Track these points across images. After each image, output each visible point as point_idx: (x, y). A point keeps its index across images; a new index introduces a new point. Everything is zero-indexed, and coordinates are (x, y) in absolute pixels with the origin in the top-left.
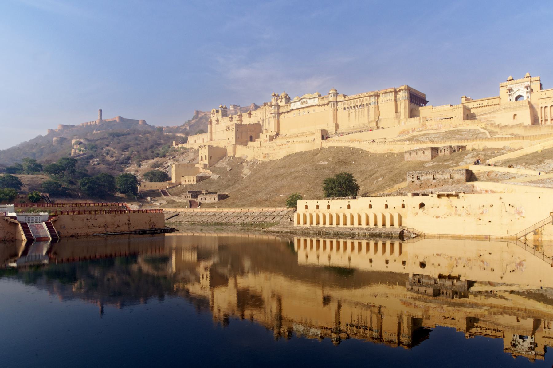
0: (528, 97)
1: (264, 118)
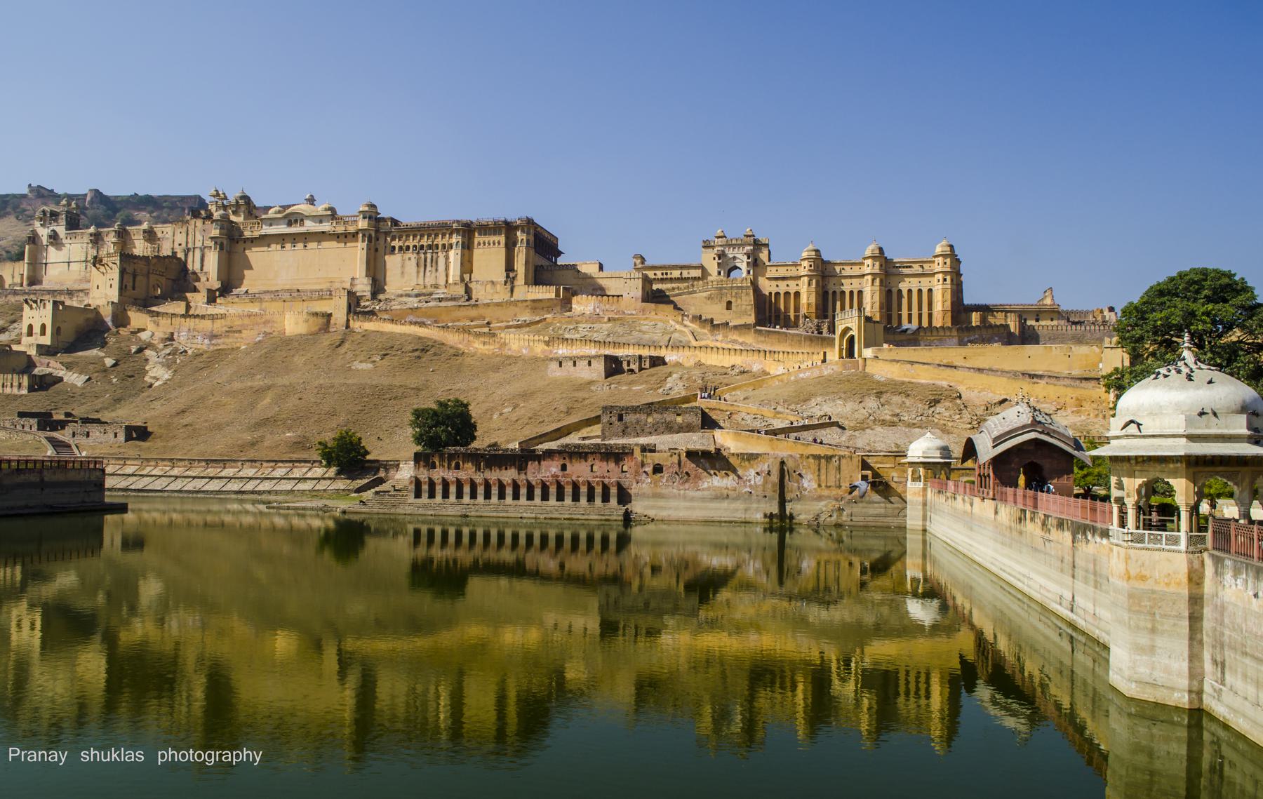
0: (749, 272)
1: (190, 245)
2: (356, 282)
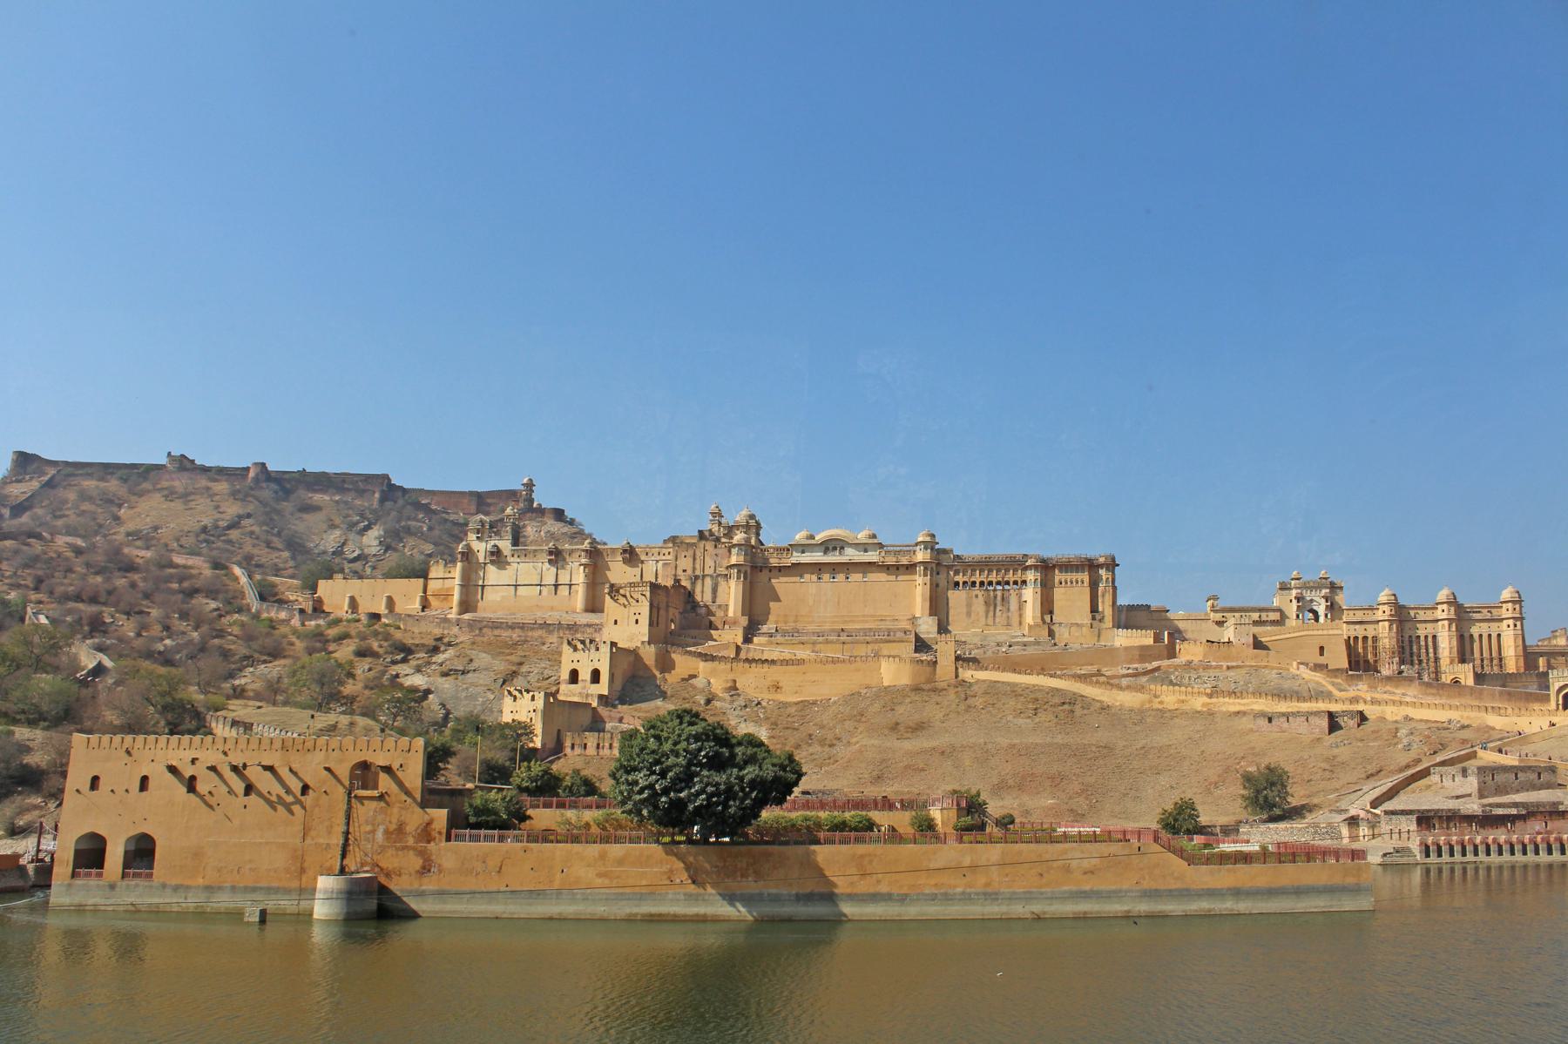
1: (698, 573)
2: (920, 622)
